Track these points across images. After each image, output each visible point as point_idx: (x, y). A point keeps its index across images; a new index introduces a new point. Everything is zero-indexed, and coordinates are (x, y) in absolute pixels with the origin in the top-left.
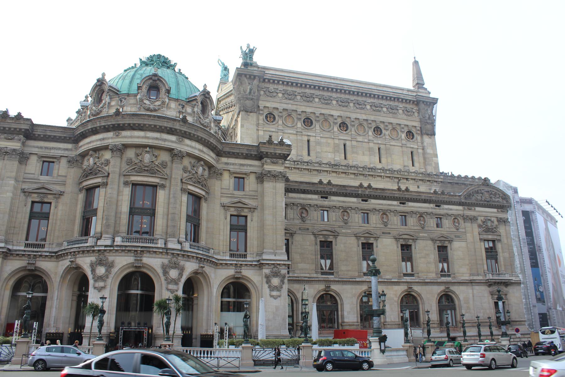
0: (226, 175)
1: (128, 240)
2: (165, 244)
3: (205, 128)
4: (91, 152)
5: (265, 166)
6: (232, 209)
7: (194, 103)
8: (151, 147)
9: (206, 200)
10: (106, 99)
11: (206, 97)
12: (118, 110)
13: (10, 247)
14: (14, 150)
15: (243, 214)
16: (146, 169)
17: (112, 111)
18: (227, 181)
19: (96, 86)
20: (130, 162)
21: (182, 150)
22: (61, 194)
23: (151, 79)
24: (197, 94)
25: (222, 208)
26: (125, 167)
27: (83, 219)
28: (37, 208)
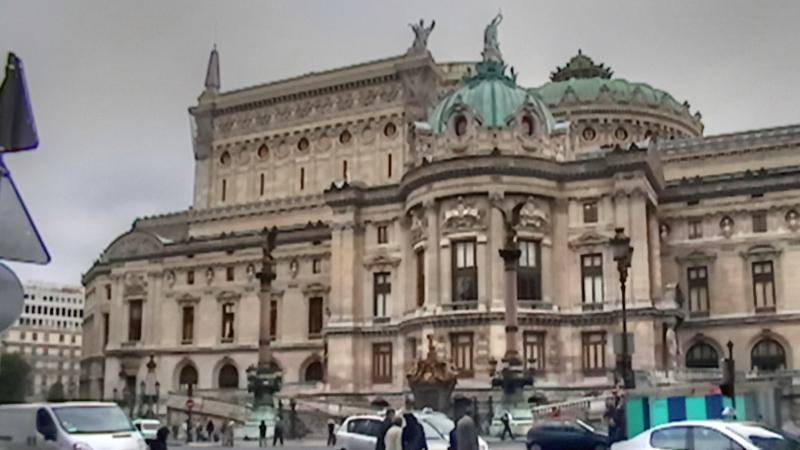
2: (488, 307)
8: (464, 196)
12: (424, 159)
13: (360, 325)
14: (349, 223)
18: (576, 212)
22: (396, 263)
28: (381, 280)
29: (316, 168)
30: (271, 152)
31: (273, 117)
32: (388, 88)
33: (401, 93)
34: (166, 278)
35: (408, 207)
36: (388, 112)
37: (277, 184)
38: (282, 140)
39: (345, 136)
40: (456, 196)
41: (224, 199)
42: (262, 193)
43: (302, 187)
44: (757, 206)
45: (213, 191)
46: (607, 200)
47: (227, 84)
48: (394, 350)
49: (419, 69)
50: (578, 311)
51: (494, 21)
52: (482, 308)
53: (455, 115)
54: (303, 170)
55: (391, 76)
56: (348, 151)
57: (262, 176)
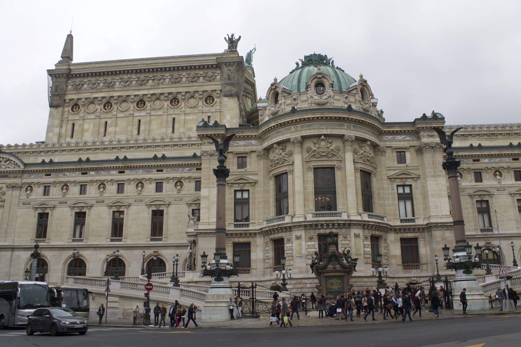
0: (389, 151)
1: (317, 215)
3: (365, 113)
4: (275, 146)
5: (423, 140)
6: (398, 180)
7: (354, 92)
8: (325, 135)
9: (375, 174)
10: (281, 100)
11: (364, 86)
15: (407, 183)
16: (324, 154)
17: (289, 109)
19: (270, 89)
20: (309, 150)
21: (352, 135)
23: (316, 77)
24: (356, 84)
25: (389, 180)
26: (306, 155)
27: (276, 201)
28: (239, 195)
29: (150, 122)
30: (115, 107)
31: (117, 83)
32: (210, 73)
33: (218, 77)
34: (24, 189)
35: (266, 144)
36: (209, 88)
37: (118, 129)
38: (125, 100)
39: (175, 100)
40: (320, 136)
41: (72, 137)
42: (105, 135)
43: (139, 133)
44: (477, 166)
45: (63, 130)
46: (412, 149)
47: (78, 58)
48: (253, 248)
49: (234, 63)
50: (398, 223)
51: (251, 51)
52: (344, 217)
53: (315, 81)
54: (140, 121)
55: (212, 65)
56: (177, 111)
57: (106, 123)
